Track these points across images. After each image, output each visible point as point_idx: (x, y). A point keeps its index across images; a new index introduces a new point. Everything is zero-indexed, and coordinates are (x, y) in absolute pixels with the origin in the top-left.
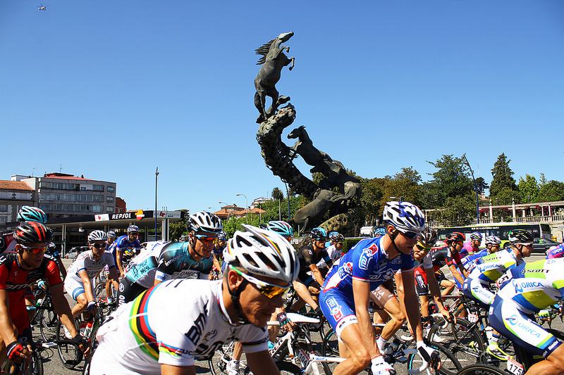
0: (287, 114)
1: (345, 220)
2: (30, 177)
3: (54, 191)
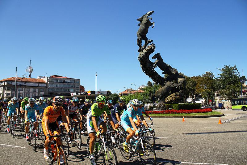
0: (151, 48)
1: (178, 95)
2: (45, 77)
3: (55, 83)
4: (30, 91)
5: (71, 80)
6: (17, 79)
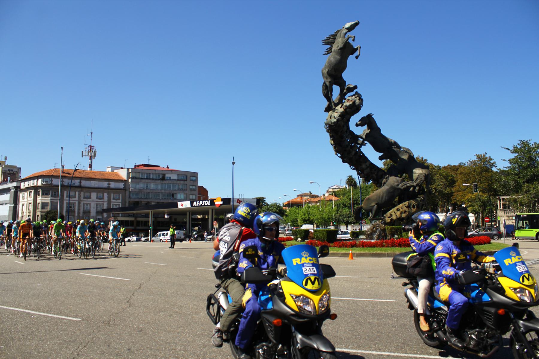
0: (354, 103)
1: (414, 207)
2: (122, 168)
3: (143, 181)
4: (90, 198)
5: (178, 175)
6: (63, 173)
